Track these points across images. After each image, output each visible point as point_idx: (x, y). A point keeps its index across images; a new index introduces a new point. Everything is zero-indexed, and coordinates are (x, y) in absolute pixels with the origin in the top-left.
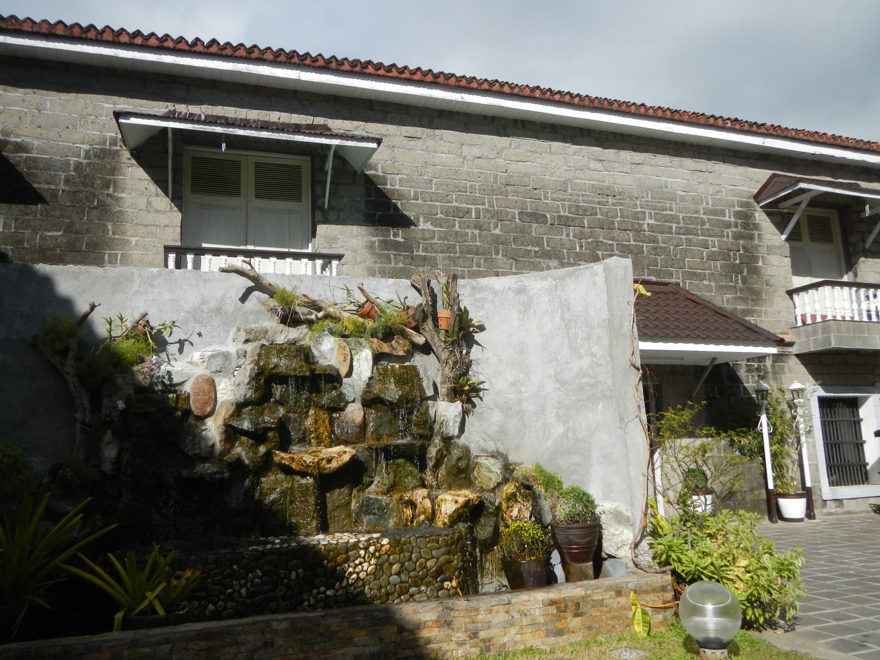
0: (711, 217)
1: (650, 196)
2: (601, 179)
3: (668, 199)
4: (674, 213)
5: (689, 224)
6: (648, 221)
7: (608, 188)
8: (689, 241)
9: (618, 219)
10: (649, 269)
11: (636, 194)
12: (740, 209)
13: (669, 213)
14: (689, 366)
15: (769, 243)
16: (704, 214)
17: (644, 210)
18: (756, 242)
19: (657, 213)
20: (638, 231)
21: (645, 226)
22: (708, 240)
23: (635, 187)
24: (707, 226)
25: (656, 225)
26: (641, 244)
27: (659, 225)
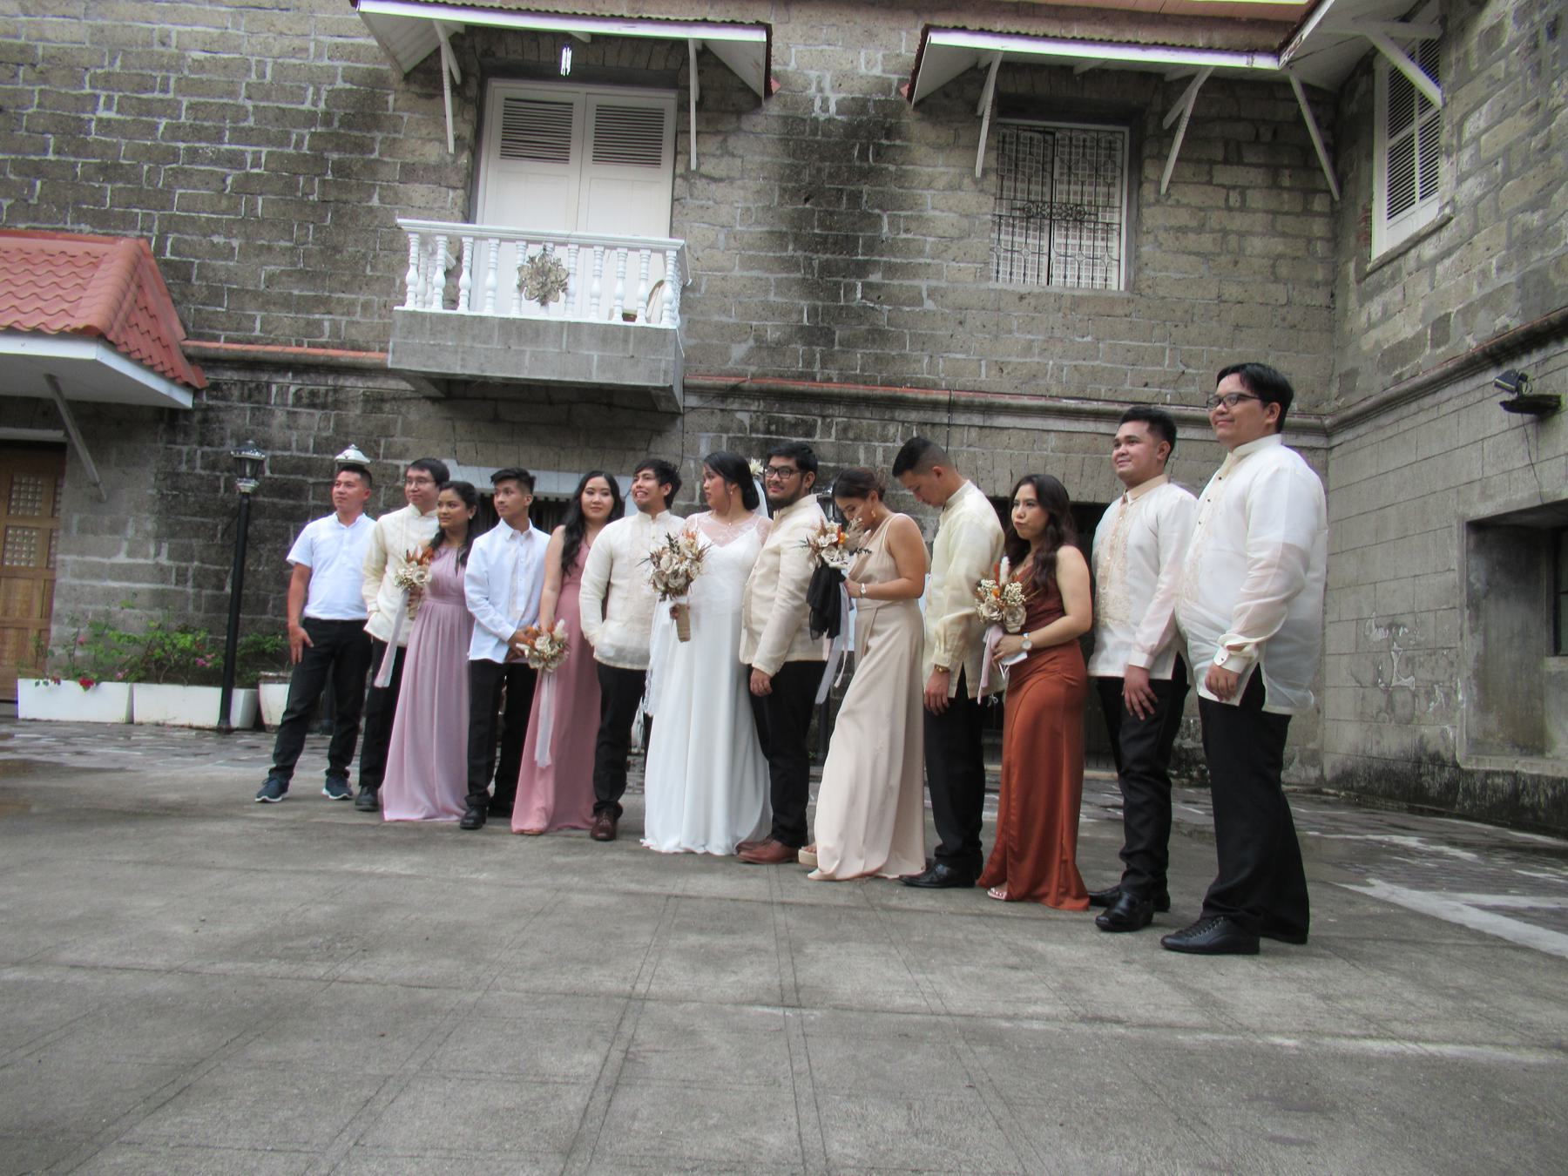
0: (262, 104)
1: (118, 63)
2: (11, 30)
3: (162, 67)
4: (170, 96)
5: (205, 120)
6: (103, 114)
7: (23, 50)
8: (193, 154)
9: (30, 111)
10: (77, 210)
11: (85, 61)
12: (348, 86)
13: (157, 95)
14: (141, 407)
15: (409, 159)
16: (249, 98)
17: (98, 92)
18: (375, 155)
19: (128, 97)
20: (72, 132)
21: (93, 124)
22: (243, 153)
23: (88, 45)
24: (251, 122)
25: (119, 121)
26: (72, 159)
27: (125, 122)
